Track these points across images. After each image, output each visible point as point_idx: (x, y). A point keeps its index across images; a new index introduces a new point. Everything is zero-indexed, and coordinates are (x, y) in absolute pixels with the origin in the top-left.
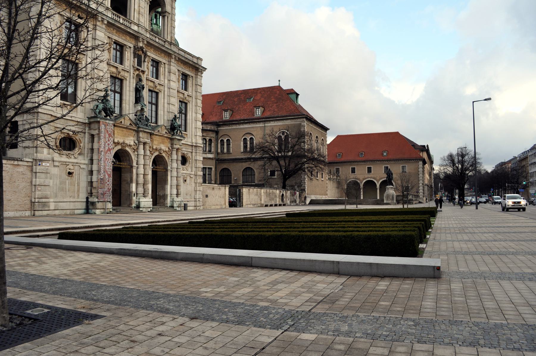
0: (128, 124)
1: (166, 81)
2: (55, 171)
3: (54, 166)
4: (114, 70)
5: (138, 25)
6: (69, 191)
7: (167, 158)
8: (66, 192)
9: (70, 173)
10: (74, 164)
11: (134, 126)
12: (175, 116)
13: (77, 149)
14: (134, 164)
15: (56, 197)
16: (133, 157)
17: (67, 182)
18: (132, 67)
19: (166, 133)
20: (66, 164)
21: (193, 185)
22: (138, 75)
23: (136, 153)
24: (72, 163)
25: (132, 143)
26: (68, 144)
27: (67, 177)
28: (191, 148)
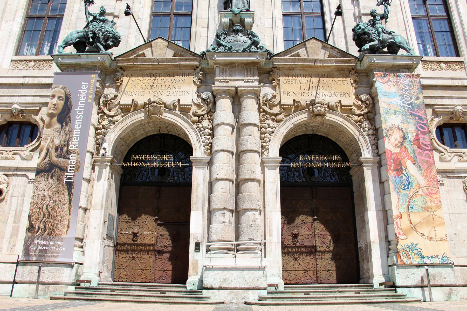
14: (199, 153)
23: (206, 123)
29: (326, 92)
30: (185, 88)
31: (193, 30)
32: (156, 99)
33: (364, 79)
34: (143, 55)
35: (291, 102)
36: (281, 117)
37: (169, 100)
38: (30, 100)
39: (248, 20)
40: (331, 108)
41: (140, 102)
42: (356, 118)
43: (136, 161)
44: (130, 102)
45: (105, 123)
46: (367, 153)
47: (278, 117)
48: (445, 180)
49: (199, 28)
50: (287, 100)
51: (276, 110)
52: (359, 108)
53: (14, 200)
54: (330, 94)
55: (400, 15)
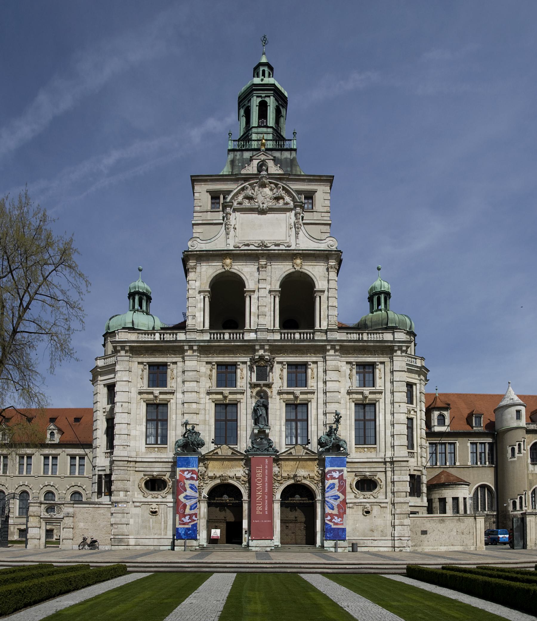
0: (230, 454)
1: (321, 385)
2: (134, 511)
3: (135, 507)
4: (220, 397)
5: (256, 331)
6: (153, 528)
7: (313, 487)
8: (150, 529)
9: (154, 513)
10: (158, 503)
11: (239, 454)
12: (331, 428)
13: (166, 489)
15: (138, 534)
16: (243, 490)
17: (151, 520)
18: (249, 386)
19: (306, 453)
20: (148, 503)
21: (389, 517)
22: (258, 394)
24: (156, 502)
25: (239, 475)
26: (154, 484)
27: (151, 516)
28: (382, 465)
29: (303, 470)
30: (238, 469)
31: (239, 432)
32: (225, 475)
33: (322, 463)
34: (217, 453)
35: (286, 475)
36: (282, 482)
37: (232, 474)
38: (160, 469)
39: (267, 431)
40: (305, 478)
41: (218, 476)
42: (316, 482)
43: (217, 500)
44: (213, 475)
45: (202, 484)
46: (319, 497)
47: (281, 482)
48: (355, 507)
49: (242, 432)
50: (285, 474)
51: (279, 478)
52: (318, 477)
53: (163, 515)
54: (305, 471)
55: (348, 421)
